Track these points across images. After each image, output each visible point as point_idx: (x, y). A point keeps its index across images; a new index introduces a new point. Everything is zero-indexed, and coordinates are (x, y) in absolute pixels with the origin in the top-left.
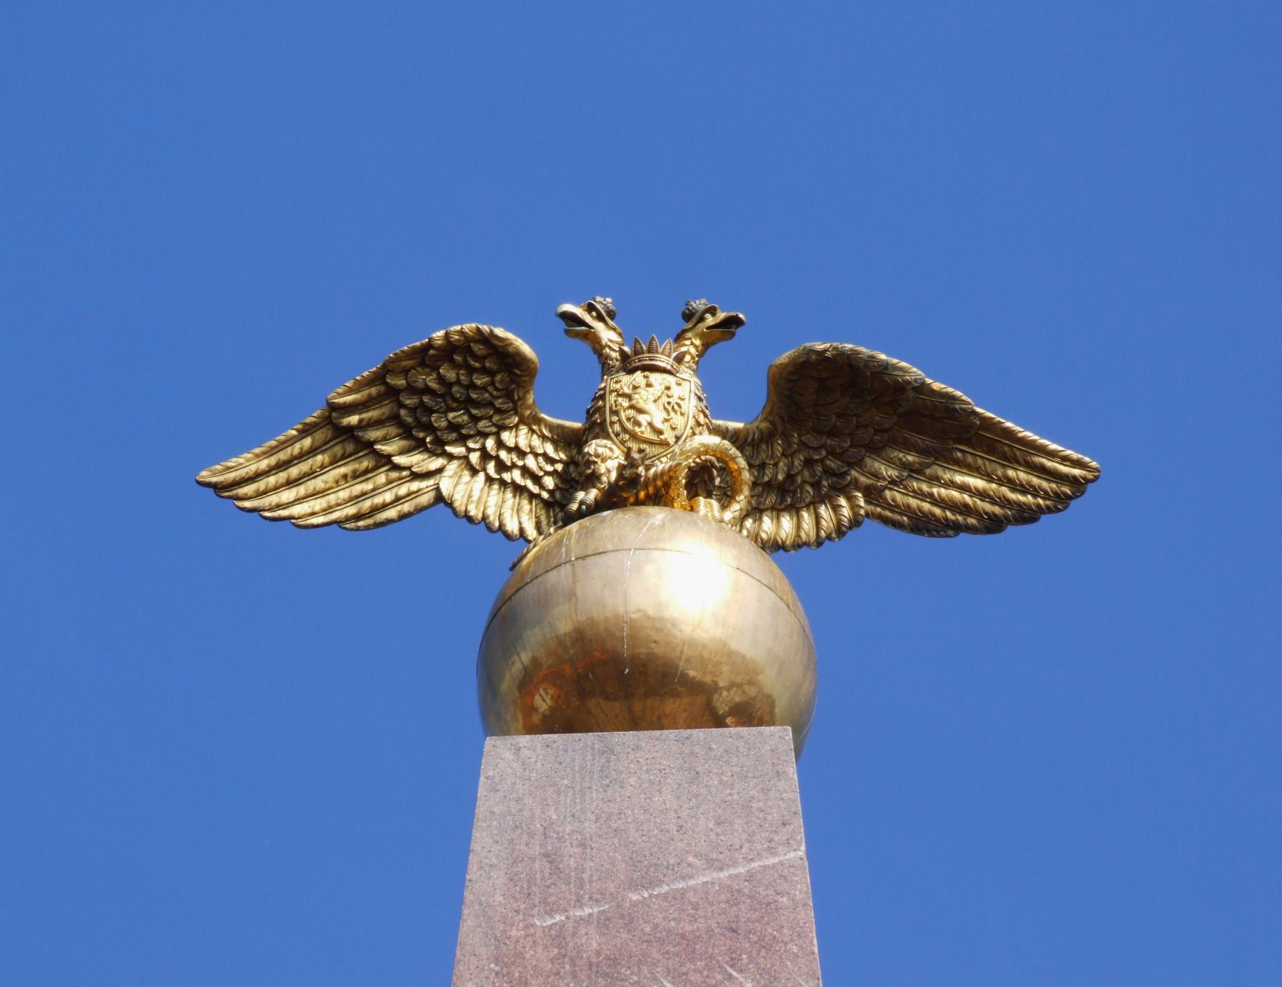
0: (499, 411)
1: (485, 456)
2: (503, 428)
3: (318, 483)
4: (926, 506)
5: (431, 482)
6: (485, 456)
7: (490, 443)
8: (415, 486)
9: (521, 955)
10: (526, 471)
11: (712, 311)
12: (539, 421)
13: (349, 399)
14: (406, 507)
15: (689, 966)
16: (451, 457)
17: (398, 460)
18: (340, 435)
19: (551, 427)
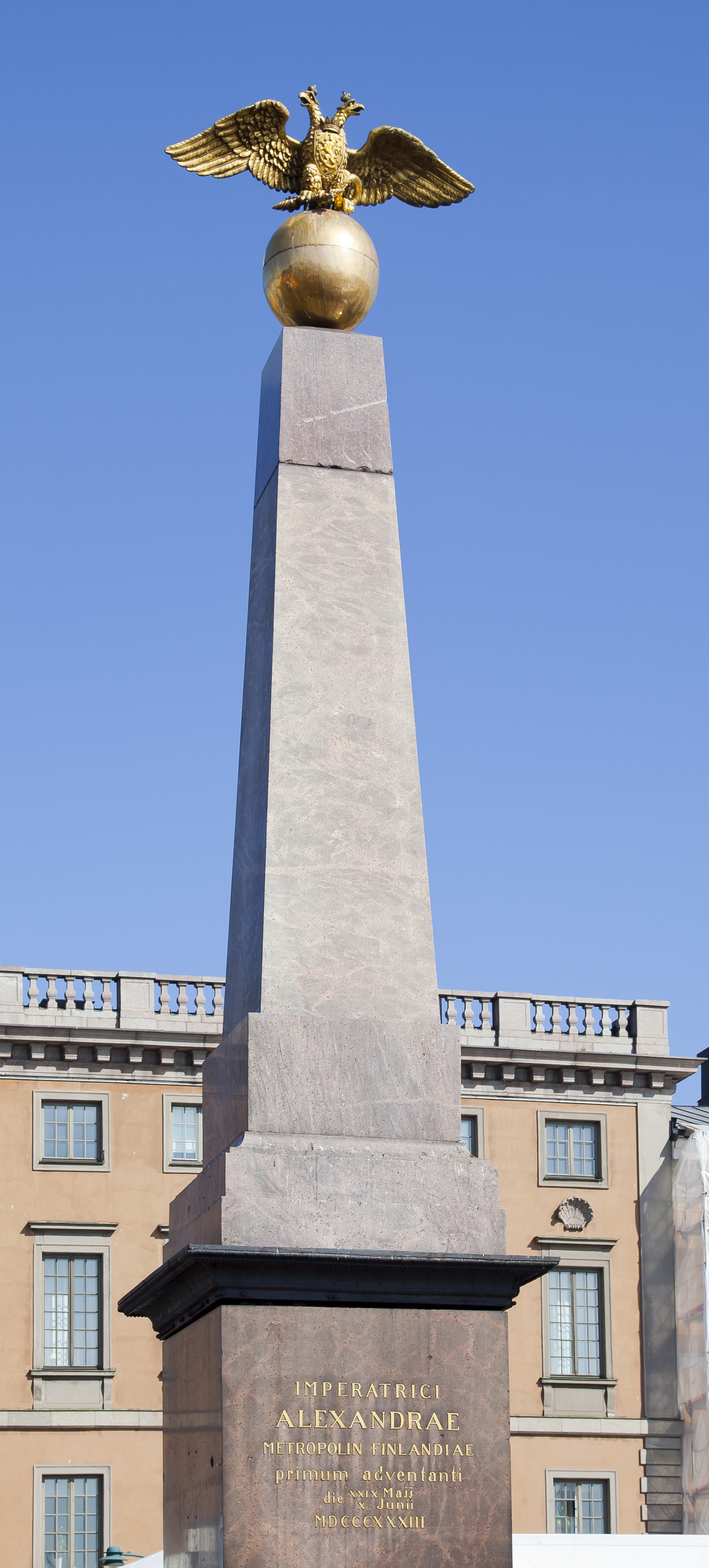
0: (272, 133)
1: (265, 151)
2: (272, 140)
3: (206, 157)
4: (414, 195)
5: (245, 161)
6: (265, 151)
7: (267, 147)
8: (240, 162)
9: (300, 435)
10: (278, 159)
11: (353, 102)
12: (286, 138)
13: (222, 125)
14: (236, 171)
15: (352, 448)
16: (253, 151)
17: (235, 151)
18: (217, 141)
19: (289, 142)
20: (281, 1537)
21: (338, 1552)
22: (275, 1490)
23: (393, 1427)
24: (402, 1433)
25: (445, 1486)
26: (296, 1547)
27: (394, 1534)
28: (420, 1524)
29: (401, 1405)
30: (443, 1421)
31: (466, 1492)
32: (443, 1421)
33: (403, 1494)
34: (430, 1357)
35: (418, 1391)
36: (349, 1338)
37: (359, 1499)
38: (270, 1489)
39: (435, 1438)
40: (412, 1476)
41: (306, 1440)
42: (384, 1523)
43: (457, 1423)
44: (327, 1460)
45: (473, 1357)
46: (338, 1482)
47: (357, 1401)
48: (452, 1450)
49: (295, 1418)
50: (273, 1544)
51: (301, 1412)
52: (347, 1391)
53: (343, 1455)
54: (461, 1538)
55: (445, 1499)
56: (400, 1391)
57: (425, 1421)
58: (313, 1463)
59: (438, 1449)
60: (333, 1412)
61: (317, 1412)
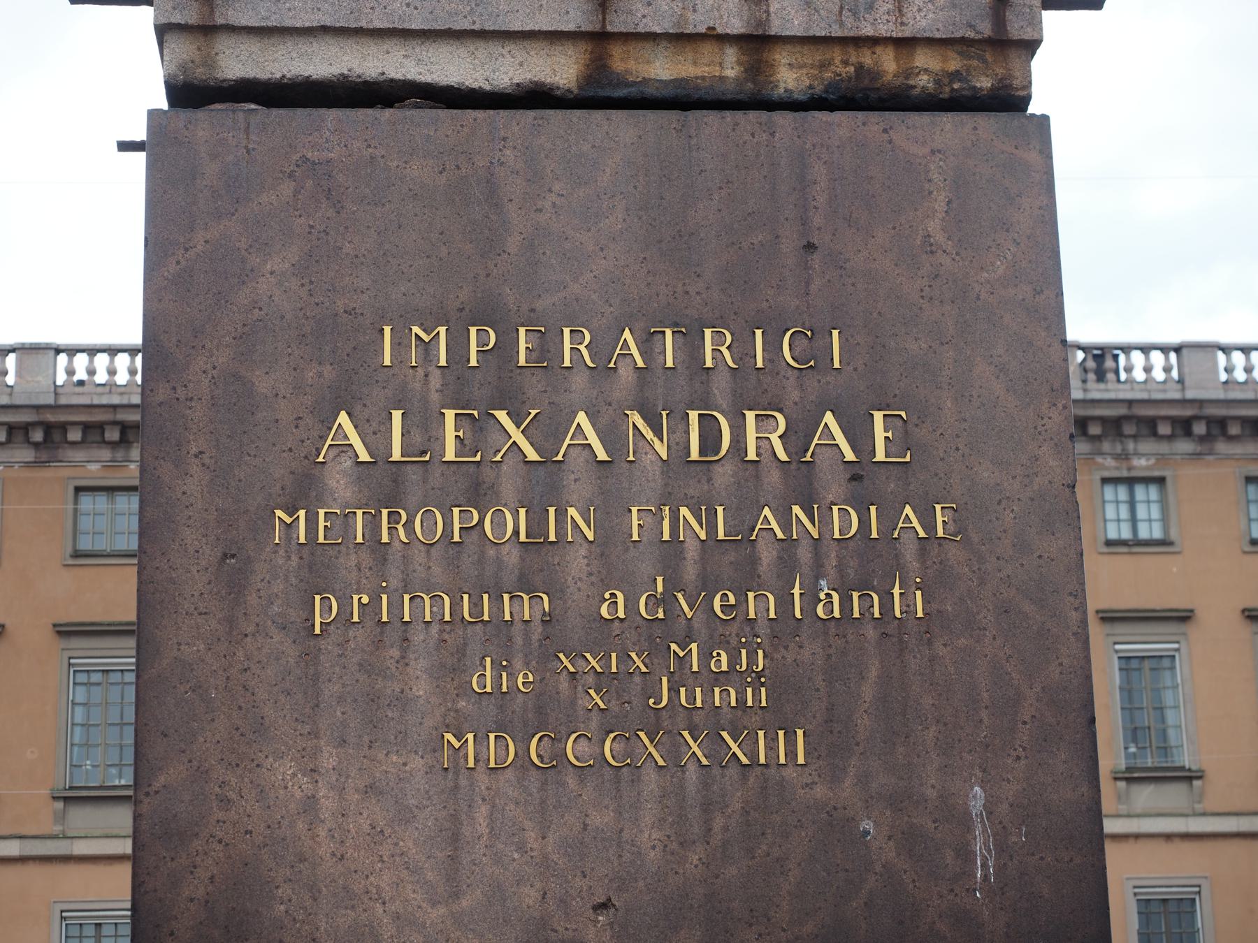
20: (328, 804)
21: (521, 848)
22: (309, 657)
23: (695, 455)
24: (724, 474)
25: (871, 633)
26: (377, 834)
27: (705, 785)
28: (791, 753)
29: (721, 387)
30: (859, 435)
31: (941, 651)
32: (859, 435)
33: (734, 660)
34: (810, 247)
35: (773, 347)
36: (553, 197)
37: (590, 679)
38: (292, 652)
39: (833, 486)
40: (761, 606)
41: (412, 500)
42: (674, 752)
43: (902, 439)
44: (481, 560)
45: (949, 246)
46: (518, 626)
47: (579, 381)
48: (890, 518)
49: (375, 434)
50: (301, 826)
51: (397, 415)
52: (546, 350)
53: (536, 543)
54: (931, 793)
55: (873, 673)
56: (715, 348)
57: (798, 436)
58: (436, 570)
59: (843, 521)
60: (502, 416)
61: (450, 415)
